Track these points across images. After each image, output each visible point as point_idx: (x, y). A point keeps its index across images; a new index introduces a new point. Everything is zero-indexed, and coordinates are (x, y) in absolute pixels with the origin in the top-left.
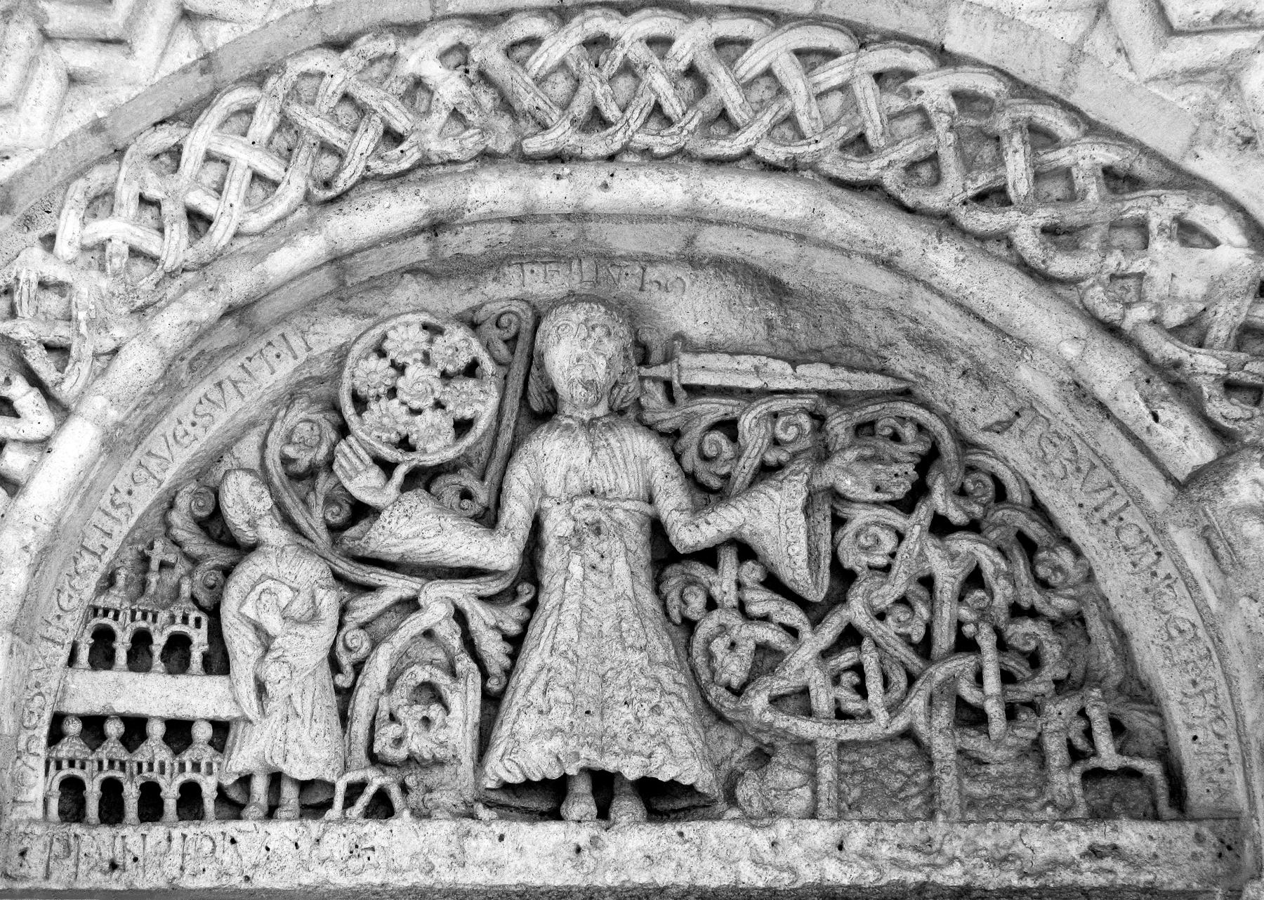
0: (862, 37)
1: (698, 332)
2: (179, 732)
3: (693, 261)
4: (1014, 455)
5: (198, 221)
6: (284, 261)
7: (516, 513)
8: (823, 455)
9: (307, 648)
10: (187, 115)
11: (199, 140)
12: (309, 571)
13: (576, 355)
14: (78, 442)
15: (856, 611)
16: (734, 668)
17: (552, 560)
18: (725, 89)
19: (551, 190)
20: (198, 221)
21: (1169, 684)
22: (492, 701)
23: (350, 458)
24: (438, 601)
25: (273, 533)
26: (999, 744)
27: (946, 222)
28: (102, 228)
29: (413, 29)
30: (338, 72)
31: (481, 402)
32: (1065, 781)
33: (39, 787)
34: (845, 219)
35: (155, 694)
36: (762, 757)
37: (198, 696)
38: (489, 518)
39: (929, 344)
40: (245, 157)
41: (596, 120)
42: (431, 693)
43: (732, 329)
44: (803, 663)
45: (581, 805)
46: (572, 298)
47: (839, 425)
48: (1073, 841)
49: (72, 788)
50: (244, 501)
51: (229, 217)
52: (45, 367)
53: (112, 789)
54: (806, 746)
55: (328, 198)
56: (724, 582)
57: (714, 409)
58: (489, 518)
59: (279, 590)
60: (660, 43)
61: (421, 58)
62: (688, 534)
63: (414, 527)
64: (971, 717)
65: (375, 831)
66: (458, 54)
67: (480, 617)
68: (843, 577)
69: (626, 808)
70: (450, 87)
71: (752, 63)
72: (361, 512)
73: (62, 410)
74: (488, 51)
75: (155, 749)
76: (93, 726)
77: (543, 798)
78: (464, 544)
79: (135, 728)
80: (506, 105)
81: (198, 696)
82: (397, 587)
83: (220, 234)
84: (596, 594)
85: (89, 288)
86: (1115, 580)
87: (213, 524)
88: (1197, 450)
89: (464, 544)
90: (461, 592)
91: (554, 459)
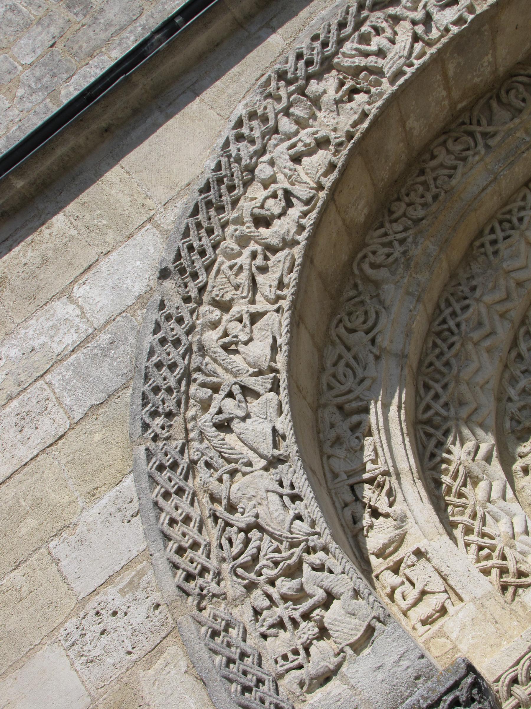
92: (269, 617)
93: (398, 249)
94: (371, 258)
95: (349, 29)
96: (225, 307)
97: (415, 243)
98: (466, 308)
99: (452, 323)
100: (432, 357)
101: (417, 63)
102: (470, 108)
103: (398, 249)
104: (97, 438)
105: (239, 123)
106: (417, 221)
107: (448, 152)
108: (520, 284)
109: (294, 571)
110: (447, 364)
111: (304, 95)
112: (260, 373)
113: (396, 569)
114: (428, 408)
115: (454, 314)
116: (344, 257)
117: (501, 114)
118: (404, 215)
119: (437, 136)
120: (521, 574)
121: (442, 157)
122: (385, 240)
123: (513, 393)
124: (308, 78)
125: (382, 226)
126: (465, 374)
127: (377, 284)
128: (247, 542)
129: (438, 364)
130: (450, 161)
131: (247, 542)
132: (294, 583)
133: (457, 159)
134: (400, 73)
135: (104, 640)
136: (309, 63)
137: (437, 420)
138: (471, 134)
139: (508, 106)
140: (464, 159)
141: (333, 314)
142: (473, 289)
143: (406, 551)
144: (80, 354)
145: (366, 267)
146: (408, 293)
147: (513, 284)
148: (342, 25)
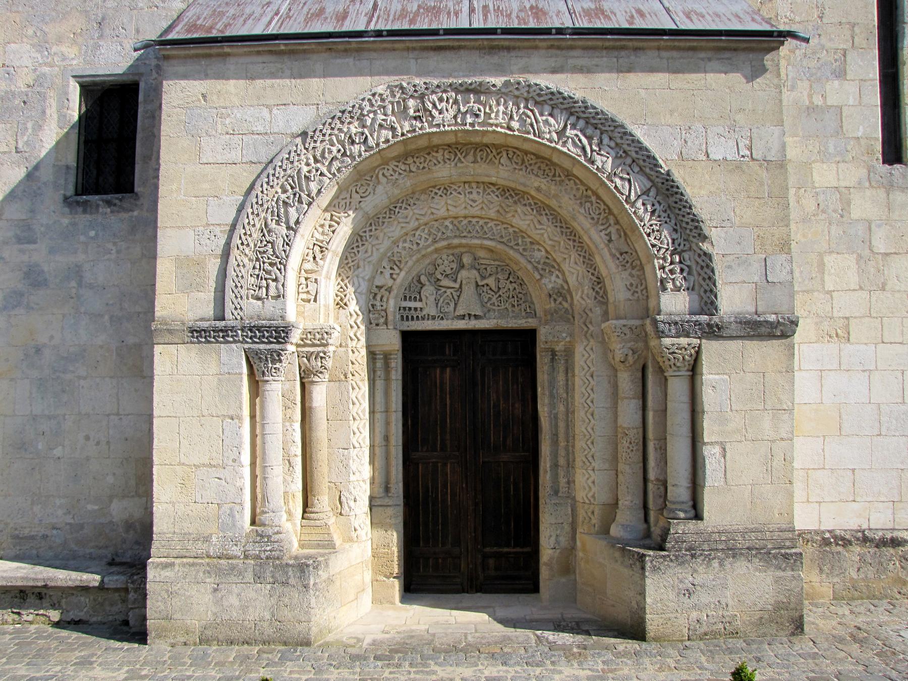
0: (503, 223)
1: (482, 256)
2: (416, 309)
3: (481, 247)
4: (520, 274)
5: (418, 244)
6: (429, 250)
7: (459, 280)
8: (497, 273)
9: (432, 298)
10: (417, 229)
11: (418, 233)
12: (432, 288)
13: (466, 260)
14: (403, 274)
15: (501, 293)
16: (486, 300)
17: (463, 286)
18: (485, 228)
19: (464, 241)
20: (418, 244)
21: (535, 302)
22: (456, 304)
23: (437, 272)
24: (449, 291)
25: (427, 283)
26: (516, 309)
27: (512, 247)
28: (405, 245)
29: (446, 219)
30: (436, 224)
31: (454, 266)
32: (524, 314)
33: (398, 316)
34: (499, 246)
35: (412, 304)
36: (489, 311)
37: (418, 305)
38: (455, 281)
39: (511, 259)
40: (424, 235)
41: (469, 232)
42: (448, 304)
43: (486, 256)
44: (494, 299)
45: (467, 318)
46: (466, 252)
47: (499, 269)
48: (524, 321)
49: (402, 316)
50: (423, 279)
51: (422, 243)
52: (398, 263)
53: (407, 317)
54: (494, 310)
55: (435, 241)
56: (485, 289)
57: (484, 266)
58: (455, 281)
59: (428, 291)
60: (478, 222)
61: (447, 223)
62: (480, 284)
63: (445, 282)
64: (513, 306)
65: (441, 322)
66: (452, 223)
67: (454, 293)
68: (499, 288)
69: (472, 318)
70: (451, 227)
71: (489, 225)
72: (438, 280)
73: (401, 270)
74: (456, 222)
75: (413, 311)
76: (405, 308)
77: (463, 317)
78: (452, 284)
79: (410, 309)
80: (458, 229)
81: (418, 305)
82: (444, 290)
83: (421, 246)
84: (469, 291)
85: (404, 253)
86: (530, 289)
87: (419, 281)
88: (538, 277)
89: (452, 284)
90: (452, 290)
91: (463, 274)
92: (257, 272)
93: (396, 176)
94: (385, 171)
95: (438, 90)
96: (316, 161)
97: (403, 178)
98: (406, 209)
99: (397, 210)
100: (381, 216)
101: (446, 128)
102: (465, 145)
103: (396, 176)
104: (245, 174)
105: (374, 95)
106: (411, 171)
107: (443, 155)
108: (432, 213)
109: (271, 264)
110: (384, 223)
111: (404, 101)
112: (308, 195)
113: (306, 279)
114: (365, 232)
115: (401, 207)
116: (375, 165)
117: (470, 158)
118: (409, 165)
119: (445, 145)
120: (345, 304)
121: (439, 156)
122: (395, 168)
123: (401, 245)
124: (412, 97)
125: (399, 162)
126: (385, 231)
127: (379, 183)
128: (265, 246)
129: (381, 220)
130: (440, 158)
131: (265, 246)
132: (270, 268)
133: (444, 160)
134: (438, 126)
135: (208, 241)
136: (416, 91)
137: (364, 238)
138: (456, 155)
139: (475, 155)
140: (445, 162)
141: (357, 181)
142: (415, 204)
143: (313, 276)
144: (260, 137)
145: (381, 173)
146: (386, 193)
147: (429, 212)
148: (438, 86)
